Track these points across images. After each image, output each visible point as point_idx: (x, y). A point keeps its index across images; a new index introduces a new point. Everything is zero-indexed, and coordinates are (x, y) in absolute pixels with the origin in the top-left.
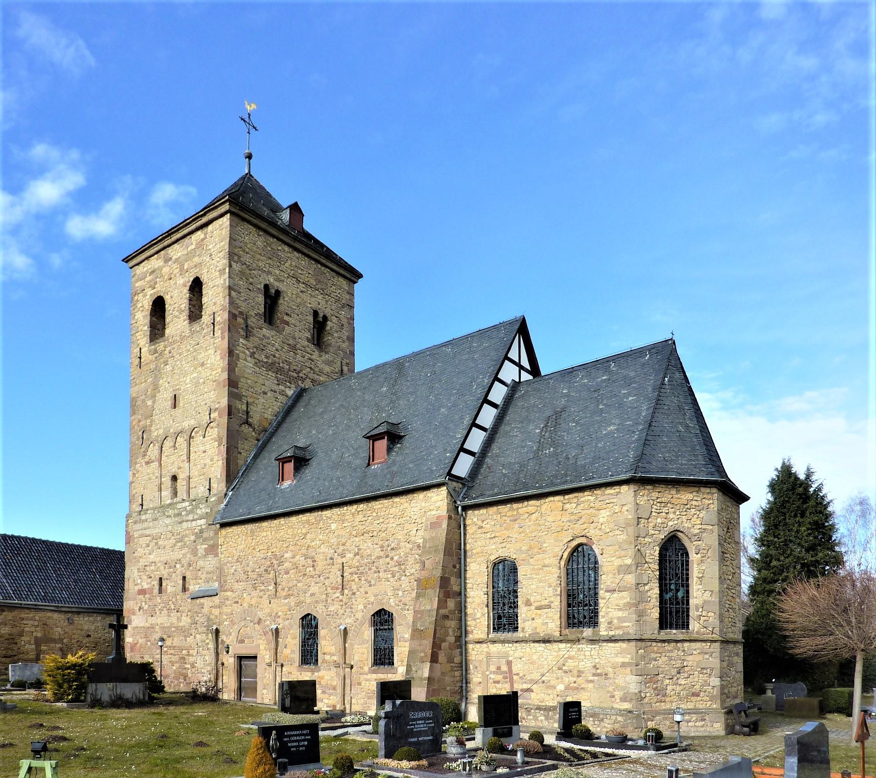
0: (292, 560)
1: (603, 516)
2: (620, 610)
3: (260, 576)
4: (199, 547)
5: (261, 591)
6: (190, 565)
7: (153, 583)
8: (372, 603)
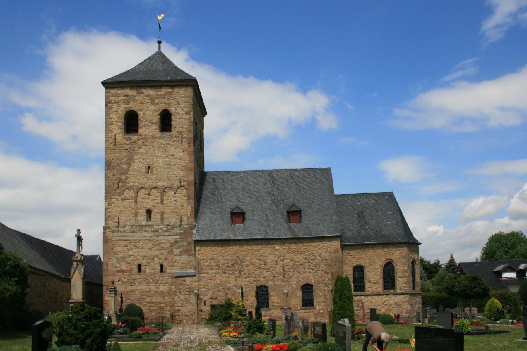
0: (251, 261)
1: (397, 253)
2: (404, 284)
3: (229, 267)
4: (175, 250)
5: (229, 274)
6: (167, 259)
7: (131, 267)
8: (301, 281)
